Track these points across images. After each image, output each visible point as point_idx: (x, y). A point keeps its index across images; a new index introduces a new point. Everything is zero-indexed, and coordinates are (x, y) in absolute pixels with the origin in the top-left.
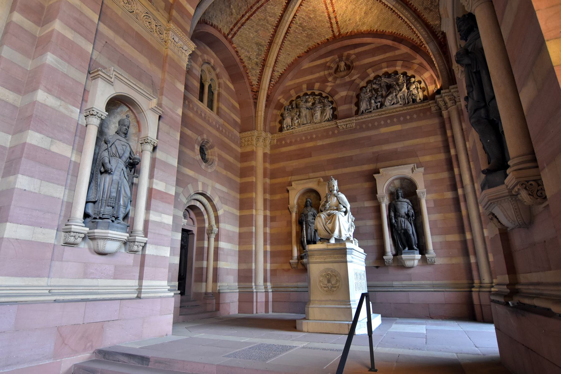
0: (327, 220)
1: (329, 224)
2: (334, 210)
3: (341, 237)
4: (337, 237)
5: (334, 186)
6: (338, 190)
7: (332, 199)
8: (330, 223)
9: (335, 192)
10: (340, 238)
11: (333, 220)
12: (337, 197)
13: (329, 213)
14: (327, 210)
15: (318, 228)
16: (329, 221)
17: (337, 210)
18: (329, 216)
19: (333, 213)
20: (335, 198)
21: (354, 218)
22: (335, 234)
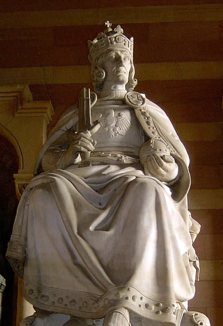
0: (89, 208)
1: (96, 229)
2: (122, 166)
3: (165, 310)
4: (142, 312)
5: (118, 61)
6: (136, 83)
7: (106, 114)
8: (107, 229)
9: (121, 91)
10: (160, 317)
11: (124, 212)
12: (132, 110)
13: (99, 174)
14: (85, 164)
15: (31, 255)
16: (103, 216)
17: (138, 165)
18: (100, 191)
19: (125, 178)
20: (126, 116)
21: (198, 227)
22: (133, 292)
